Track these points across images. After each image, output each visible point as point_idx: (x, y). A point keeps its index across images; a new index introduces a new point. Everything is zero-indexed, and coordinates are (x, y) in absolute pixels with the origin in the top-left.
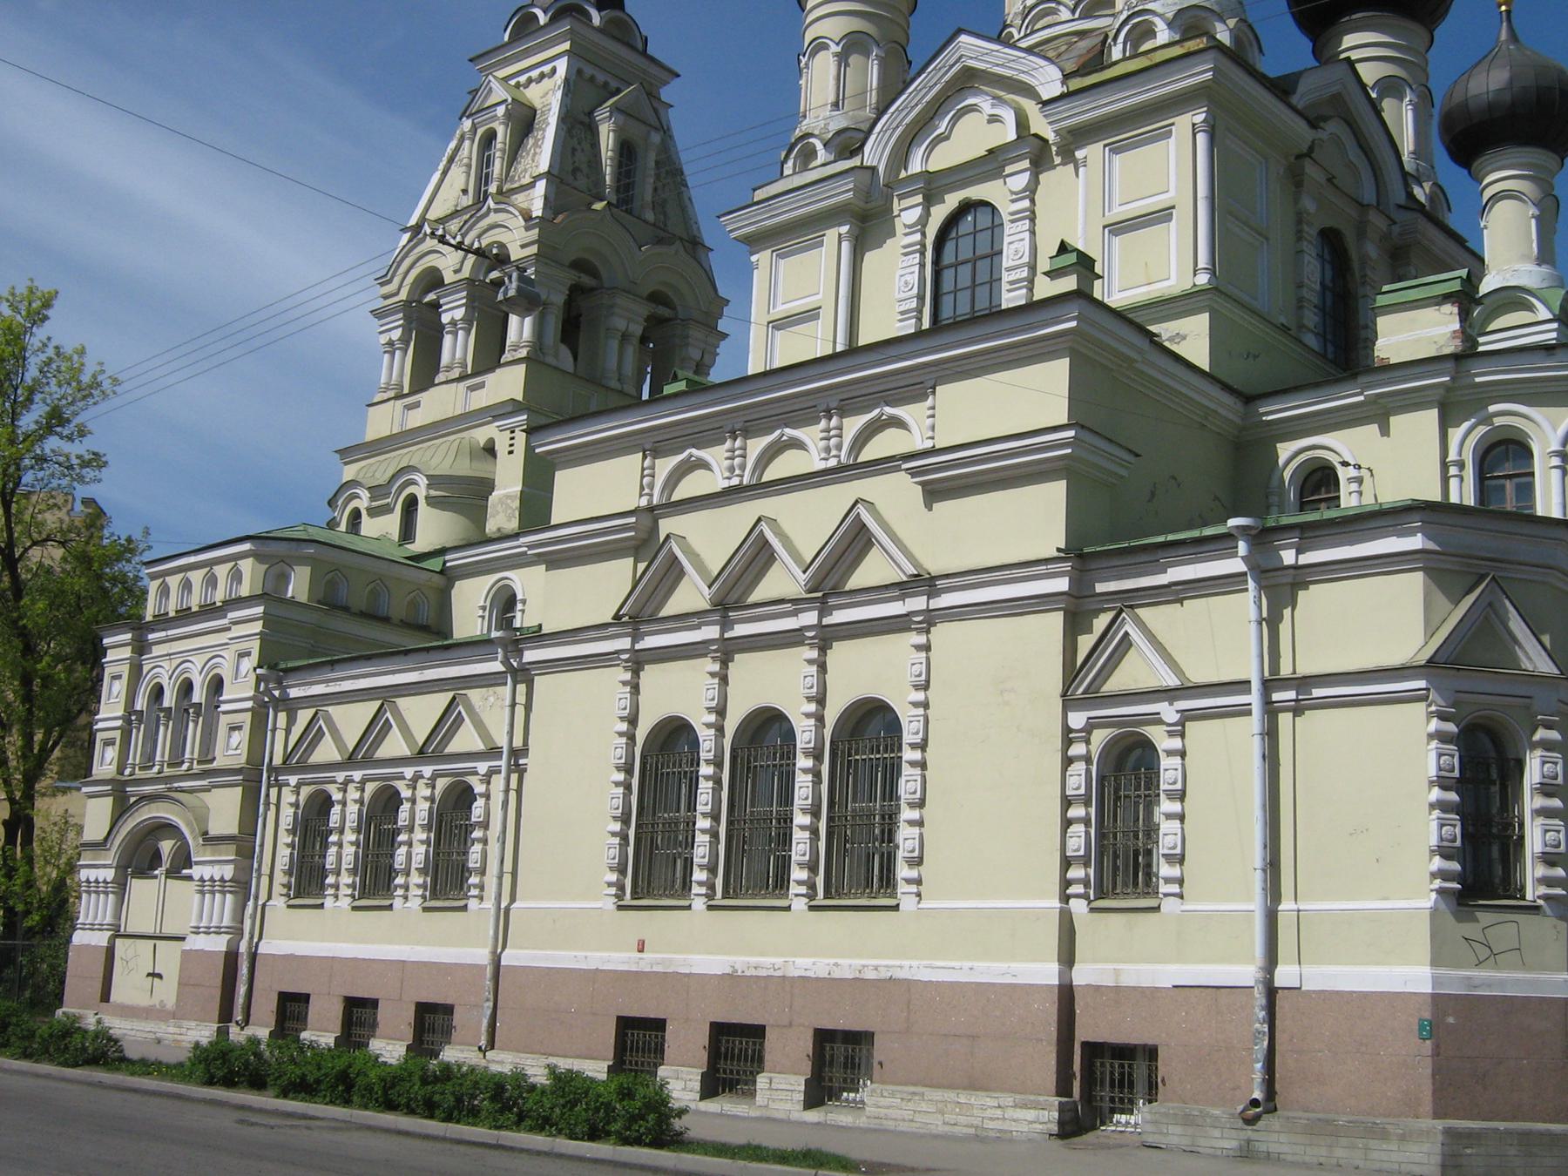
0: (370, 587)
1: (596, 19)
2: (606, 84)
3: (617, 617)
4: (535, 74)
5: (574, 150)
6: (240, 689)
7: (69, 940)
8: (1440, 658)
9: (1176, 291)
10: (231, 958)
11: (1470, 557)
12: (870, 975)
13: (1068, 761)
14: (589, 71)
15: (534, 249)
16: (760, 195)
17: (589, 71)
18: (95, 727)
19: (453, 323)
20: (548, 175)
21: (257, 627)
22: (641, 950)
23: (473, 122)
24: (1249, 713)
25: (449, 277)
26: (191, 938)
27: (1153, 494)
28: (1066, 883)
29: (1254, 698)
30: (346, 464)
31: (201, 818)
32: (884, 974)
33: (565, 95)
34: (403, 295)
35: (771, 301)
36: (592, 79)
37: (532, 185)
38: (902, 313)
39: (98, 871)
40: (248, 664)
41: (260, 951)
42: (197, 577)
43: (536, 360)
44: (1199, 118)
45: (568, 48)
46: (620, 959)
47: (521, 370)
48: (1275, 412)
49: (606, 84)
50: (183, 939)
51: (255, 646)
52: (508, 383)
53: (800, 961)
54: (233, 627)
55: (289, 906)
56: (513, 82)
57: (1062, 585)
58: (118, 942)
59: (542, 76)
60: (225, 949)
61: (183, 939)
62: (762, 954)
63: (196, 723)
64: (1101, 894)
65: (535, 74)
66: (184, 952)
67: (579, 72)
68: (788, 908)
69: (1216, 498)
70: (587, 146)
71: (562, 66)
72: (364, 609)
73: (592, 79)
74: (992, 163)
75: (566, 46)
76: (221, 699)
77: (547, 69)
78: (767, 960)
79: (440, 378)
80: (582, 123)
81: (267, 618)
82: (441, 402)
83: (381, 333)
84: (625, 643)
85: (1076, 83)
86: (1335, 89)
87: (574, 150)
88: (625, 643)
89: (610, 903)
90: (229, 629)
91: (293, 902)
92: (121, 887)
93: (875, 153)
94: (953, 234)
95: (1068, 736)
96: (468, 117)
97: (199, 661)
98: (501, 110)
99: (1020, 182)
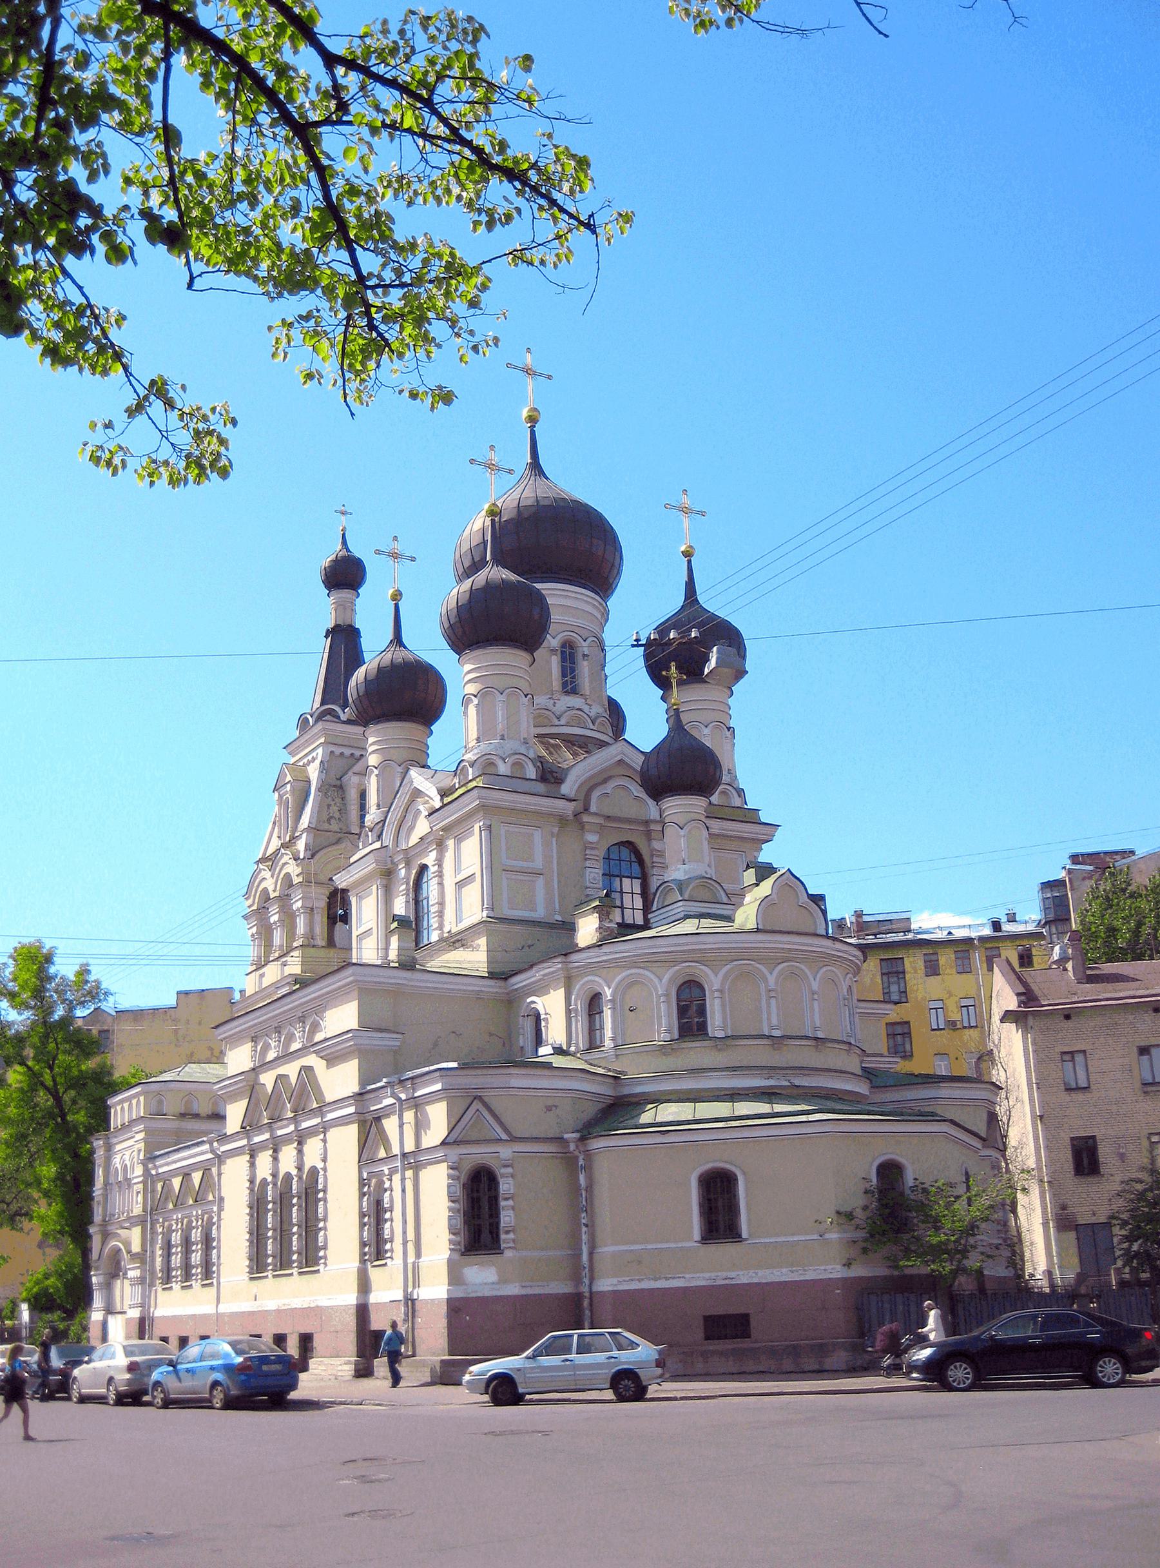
0: (212, 1101)
1: (343, 717)
2: (352, 754)
3: (242, 1128)
5: (329, 806)
6: (139, 1170)
7: (90, 1317)
12: (312, 1305)
14: (338, 750)
16: (352, 860)
17: (338, 750)
21: (141, 1135)
28: (363, 1254)
31: (128, 1244)
36: (342, 754)
40: (142, 1157)
41: (156, 1315)
43: (308, 946)
46: (245, 1306)
48: (519, 981)
51: (142, 1145)
55: (163, 1289)
56: (301, 764)
57: (352, 1110)
59: (314, 759)
65: (310, 757)
66: (127, 1320)
68: (385, 1265)
69: (491, 1035)
70: (338, 800)
71: (320, 751)
73: (342, 754)
77: (314, 754)
80: (335, 786)
81: (146, 1130)
82: (272, 973)
84: (244, 1142)
85: (447, 800)
86: (618, 758)
87: (329, 806)
88: (244, 1142)
89: (246, 1277)
94: (425, 880)
95: (362, 1183)
97: (128, 1153)
98: (288, 786)
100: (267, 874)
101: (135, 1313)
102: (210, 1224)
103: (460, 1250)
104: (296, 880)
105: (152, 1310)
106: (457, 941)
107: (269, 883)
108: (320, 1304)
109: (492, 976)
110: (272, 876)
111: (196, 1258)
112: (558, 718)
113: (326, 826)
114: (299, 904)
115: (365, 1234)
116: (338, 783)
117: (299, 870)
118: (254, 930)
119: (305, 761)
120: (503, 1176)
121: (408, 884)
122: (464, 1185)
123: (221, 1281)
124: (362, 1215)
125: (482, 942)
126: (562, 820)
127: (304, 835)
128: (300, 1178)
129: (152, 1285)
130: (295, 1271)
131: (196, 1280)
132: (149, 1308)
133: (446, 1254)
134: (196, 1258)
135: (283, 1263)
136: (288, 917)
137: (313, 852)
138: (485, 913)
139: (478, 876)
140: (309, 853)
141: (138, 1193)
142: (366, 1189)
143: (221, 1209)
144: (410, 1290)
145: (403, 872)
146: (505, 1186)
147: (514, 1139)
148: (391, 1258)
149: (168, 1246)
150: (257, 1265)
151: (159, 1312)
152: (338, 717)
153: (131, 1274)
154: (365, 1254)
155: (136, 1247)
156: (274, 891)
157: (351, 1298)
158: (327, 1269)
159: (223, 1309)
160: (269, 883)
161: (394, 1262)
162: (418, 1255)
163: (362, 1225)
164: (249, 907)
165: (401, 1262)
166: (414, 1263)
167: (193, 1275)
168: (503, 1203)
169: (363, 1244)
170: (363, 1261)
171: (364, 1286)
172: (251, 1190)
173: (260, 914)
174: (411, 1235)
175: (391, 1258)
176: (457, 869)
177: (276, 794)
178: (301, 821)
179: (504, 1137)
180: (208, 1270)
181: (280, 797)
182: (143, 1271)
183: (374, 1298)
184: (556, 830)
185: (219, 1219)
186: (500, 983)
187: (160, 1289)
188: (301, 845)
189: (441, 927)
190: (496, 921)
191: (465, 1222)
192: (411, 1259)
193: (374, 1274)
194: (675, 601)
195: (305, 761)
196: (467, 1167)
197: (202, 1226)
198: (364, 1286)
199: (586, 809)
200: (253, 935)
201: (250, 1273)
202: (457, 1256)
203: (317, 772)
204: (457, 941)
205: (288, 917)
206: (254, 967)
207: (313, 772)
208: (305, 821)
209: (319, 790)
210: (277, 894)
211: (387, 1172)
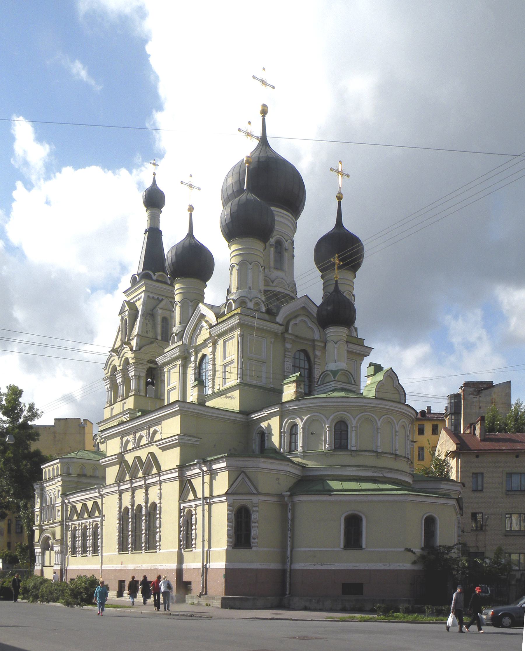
1: (154, 278)
2: (158, 298)
4: (137, 298)
5: (147, 324)
7: (34, 568)
8: (230, 492)
9: (234, 384)
10: (61, 570)
11: (237, 467)
13: (180, 517)
15: (133, 361)
17: (151, 295)
18: (56, 506)
19: (119, 383)
20: (137, 335)
22: (122, 564)
23: (122, 316)
24: (201, 505)
25: (118, 368)
26: (54, 566)
27: (215, 446)
28: (180, 545)
29: (201, 502)
30: (100, 427)
32: (155, 568)
33: (143, 306)
34: (109, 374)
35: (169, 384)
36: (153, 297)
37: (133, 339)
38: (192, 387)
39: (38, 550)
41: (68, 569)
42: (51, 468)
43: (137, 395)
44: (239, 333)
45: (144, 290)
46: (118, 566)
47: (133, 397)
48: (255, 416)
49: (158, 298)
50: (53, 566)
52: (130, 403)
53: (144, 565)
54: (57, 483)
58: (44, 568)
59: (139, 299)
60: (60, 568)
61: (53, 566)
62: (138, 564)
63: (48, 511)
64: (187, 548)
65: (137, 298)
67: (148, 296)
71: (143, 295)
72: (91, 475)
73: (153, 297)
74: (204, 344)
75: (144, 289)
76: (35, 508)
77: (139, 296)
78: (139, 565)
79: (118, 400)
80: (150, 314)
82: (118, 408)
83: (106, 385)
86: (303, 305)
89: (116, 553)
90: (56, 484)
91: (72, 556)
92: (43, 554)
93: (186, 340)
95: (180, 511)
96: (121, 314)
98: (127, 313)
99: (211, 349)
100: (115, 358)
101: (58, 567)
102: (96, 527)
103: (232, 546)
104: (131, 361)
105: (66, 566)
106: (221, 394)
107: (117, 362)
108: (157, 568)
109: (241, 412)
110: (119, 358)
111: (89, 543)
112: (273, 283)
113: (145, 335)
114: (133, 373)
115: (181, 536)
116: (151, 312)
117: (133, 356)
118: (108, 386)
119: (135, 299)
120: (253, 511)
121: (196, 364)
122: (234, 514)
123: (103, 555)
124: (180, 527)
125: (236, 394)
126: (276, 335)
127: (136, 338)
128: (133, 510)
129: (66, 554)
130: (143, 551)
131: (79, 554)
132: (65, 565)
133: (225, 547)
134: (89, 543)
135: (136, 547)
136: (126, 380)
137: (140, 347)
138: (238, 381)
139: (236, 361)
140: (138, 347)
141: (58, 511)
142: (182, 514)
143: (102, 520)
144: (205, 563)
145: (193, 358)
146: (254, 516)
147: (259, 494)
148: (195, 548)
149: (74, 537)
150: (123, 547)
151: (70, 567)
152: (152, 278)
153: (55, 549)
154: (181, 545)
155: (58, 536)
156: (120, 366)
157: (174, 566)
158: (161, 551)
159: (104, 567)
160: (117, 362)
161: (197, 550)
162: (210, 547)
163: (180, 532)
164: (106, 374)
165: (201, 550)
166: (207, 551)
167: (77, 552)
168: (253, 525)
169: (180, 541)
170: (180, 549)
171: (180, 560)
172: (120, 511)
173: (112, 378)
174: (206, 537)
175: (195, 548)
176: (224, 357)
177: (120, 316)
178: (133, 331)
179: (255, 492)
180: (96, 550)
181: (122, 318)
182: (62, 548)
183: (184, 566)
184: (273, 340)
185: (102, 526)
186: (245, 417)
187: (70, 557)
188: (134, 343)
189: (213, 387)
190: (243, 386)
191: (234, 533)
192: (206, 549)
193: (186, 555)
194: (330, 225)
195: (135, 299)
196: (237, 506)
197: (82, 529)
198: (180, 560)
199: (287, 330)
200: (108, 389)
201: (119, 551)
202: (230, 549)
203: (142, 305)
204: (221, 394)
205: (126, 380)
206: (108, 405)
207: (139, 305)
208: (136, 331)
209: (142, 315)
210: (121, 368)
211: (194, 506)
